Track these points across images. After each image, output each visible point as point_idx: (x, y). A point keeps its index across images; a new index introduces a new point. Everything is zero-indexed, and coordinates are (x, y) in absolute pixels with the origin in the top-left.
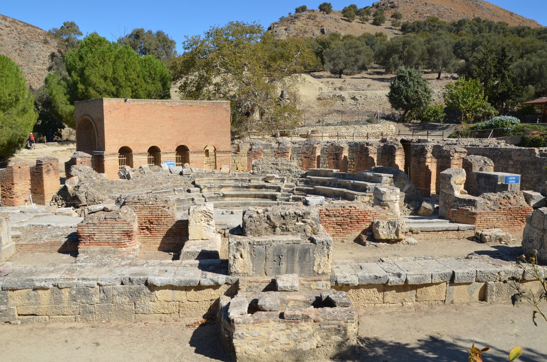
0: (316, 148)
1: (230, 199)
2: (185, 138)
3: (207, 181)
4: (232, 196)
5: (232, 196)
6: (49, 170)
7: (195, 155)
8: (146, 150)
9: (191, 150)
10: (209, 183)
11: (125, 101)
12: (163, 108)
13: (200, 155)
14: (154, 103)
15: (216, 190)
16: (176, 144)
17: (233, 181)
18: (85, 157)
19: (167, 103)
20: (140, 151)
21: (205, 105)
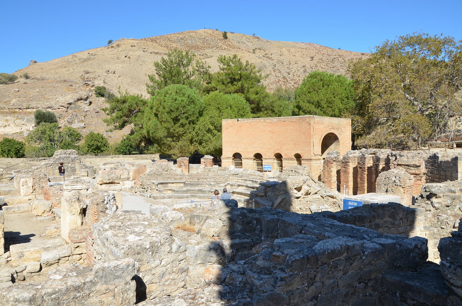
0: (366, 158)
1: (237, 195)
2: (280, 147)
3: (237, 180)
4: (238, 193)
5: (238, 193)
6: (181, 166)
7: (287, 161)
8: (252, 156)
9: (284, 157)
10: (237, 182)
11: (238, 120)
12: (265, 124)
13: (290, 162)
14: (258, 120)
15: (236, 187)
16: (274, 152)
17: (251, 182)
18: (207, 159)
19: (267, 120)
20: (247, 157)
21: (294, 120)
